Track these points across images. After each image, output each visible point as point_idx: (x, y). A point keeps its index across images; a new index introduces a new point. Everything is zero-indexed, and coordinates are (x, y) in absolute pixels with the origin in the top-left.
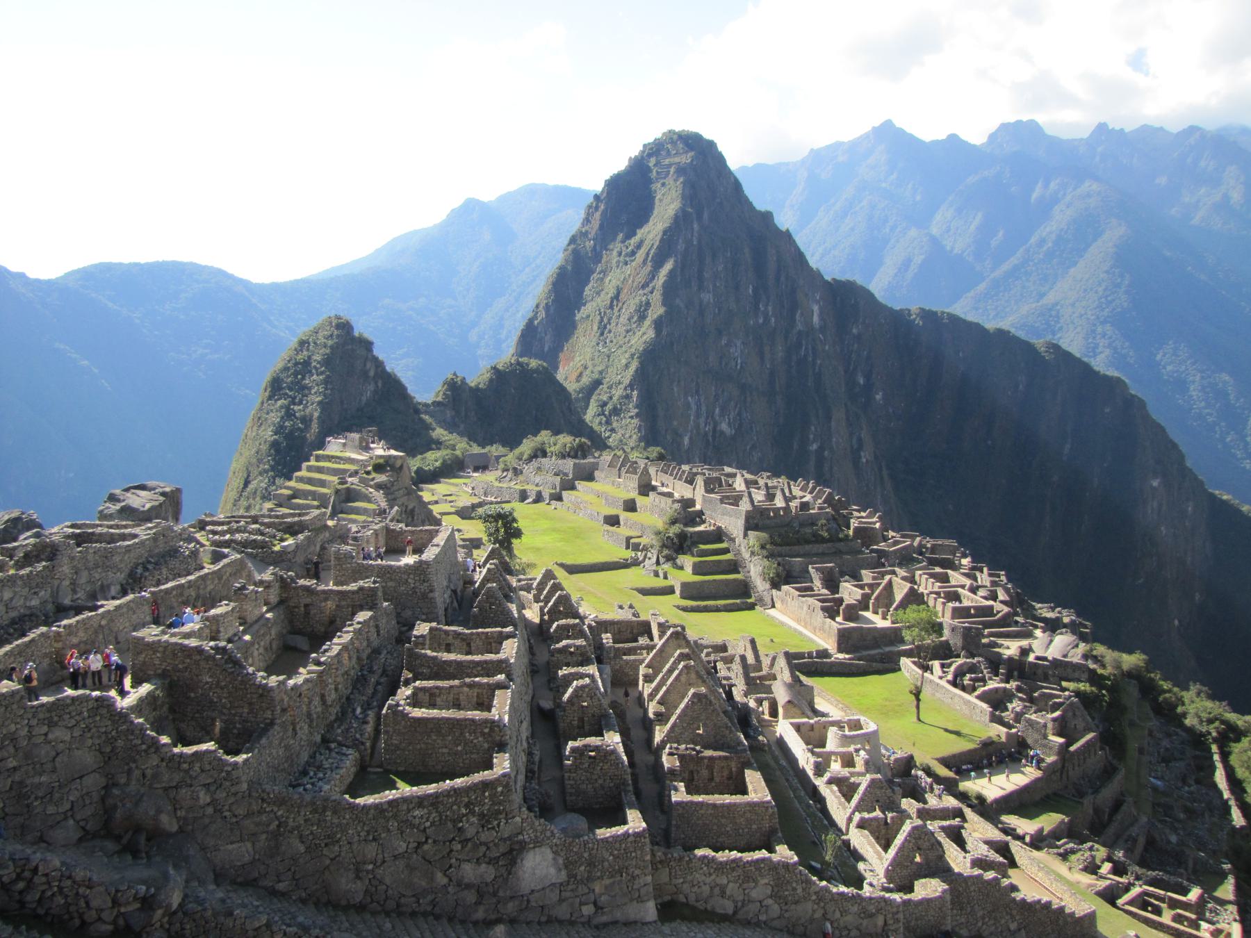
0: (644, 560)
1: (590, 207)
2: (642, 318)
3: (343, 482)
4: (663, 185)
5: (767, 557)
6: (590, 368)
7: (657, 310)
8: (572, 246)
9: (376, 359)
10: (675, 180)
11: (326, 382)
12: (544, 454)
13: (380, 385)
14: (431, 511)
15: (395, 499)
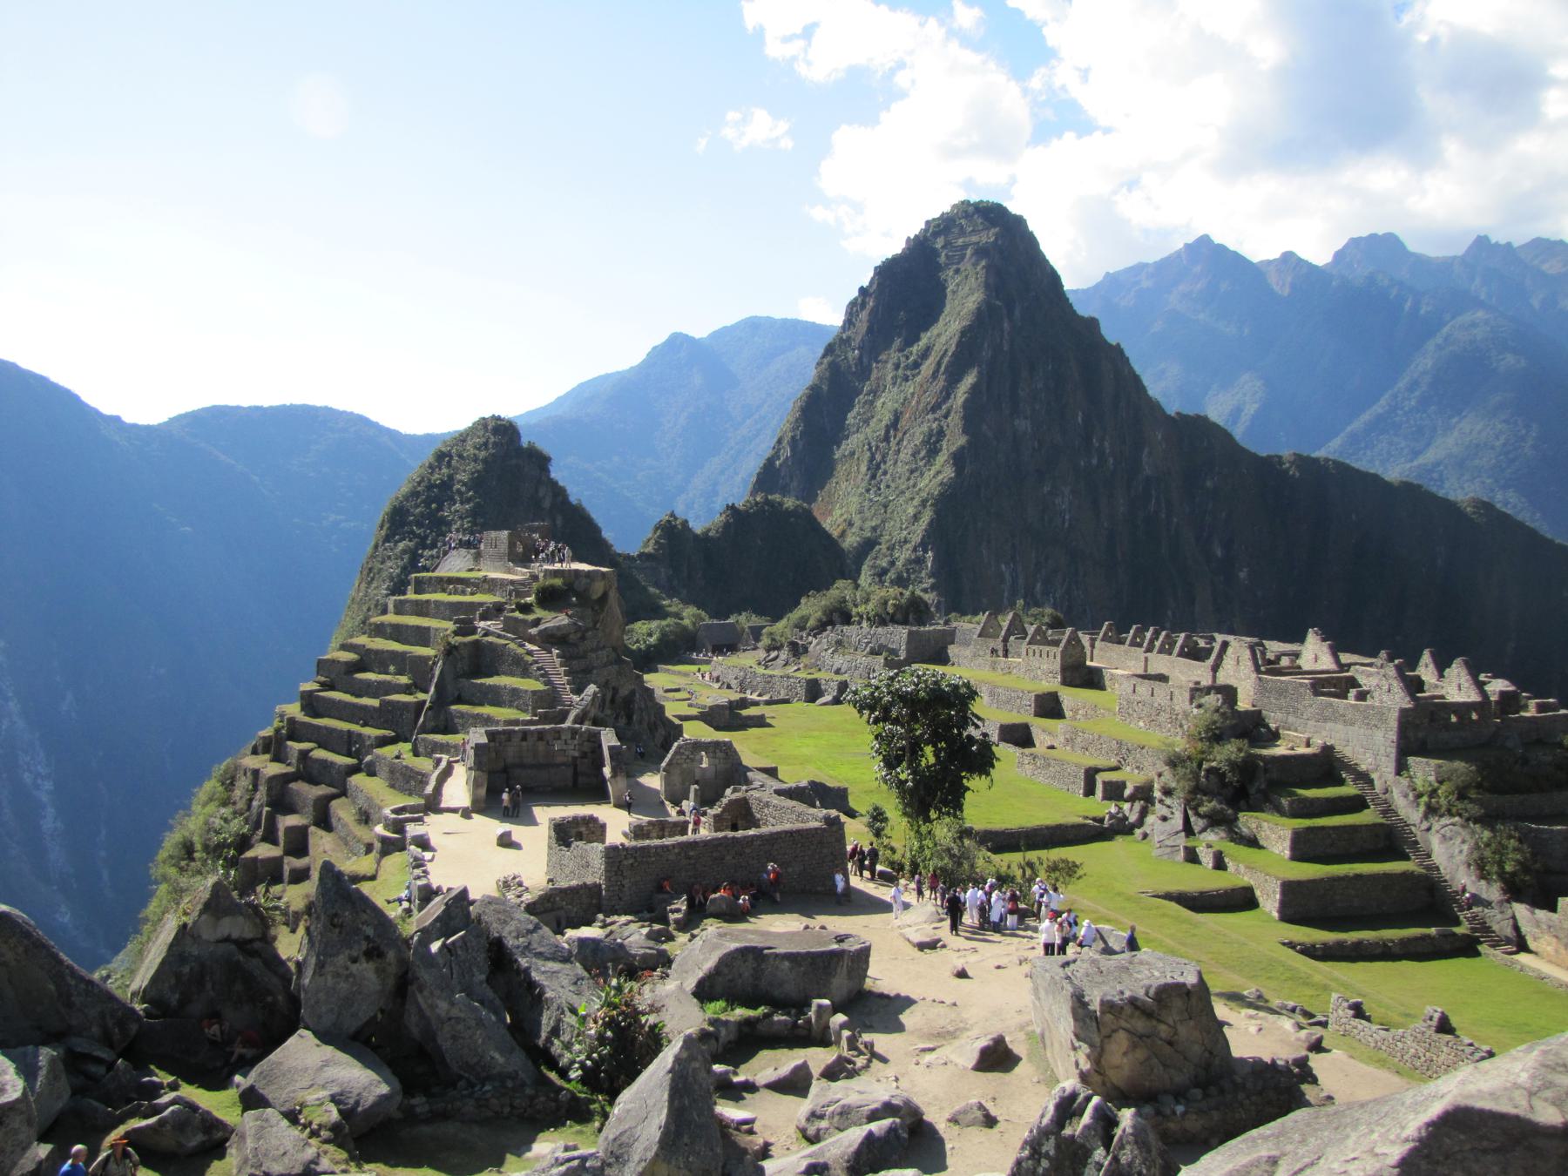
0: (1140, 822)
1: (853, 304)
2: (933, 452)
3: (466, 628)
4: (957, 271)
5: (1486, 820)
6: (858, 523)
7: (955, 440)
8: (829, 358)
9: (554, 484)
10: (975, 265)
11: (474, 514)
12: (847, 619)
13: (559, 522)
14: (662, 708)
15: (587, 671)
